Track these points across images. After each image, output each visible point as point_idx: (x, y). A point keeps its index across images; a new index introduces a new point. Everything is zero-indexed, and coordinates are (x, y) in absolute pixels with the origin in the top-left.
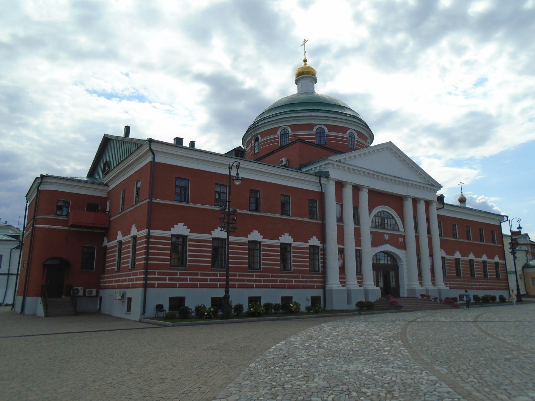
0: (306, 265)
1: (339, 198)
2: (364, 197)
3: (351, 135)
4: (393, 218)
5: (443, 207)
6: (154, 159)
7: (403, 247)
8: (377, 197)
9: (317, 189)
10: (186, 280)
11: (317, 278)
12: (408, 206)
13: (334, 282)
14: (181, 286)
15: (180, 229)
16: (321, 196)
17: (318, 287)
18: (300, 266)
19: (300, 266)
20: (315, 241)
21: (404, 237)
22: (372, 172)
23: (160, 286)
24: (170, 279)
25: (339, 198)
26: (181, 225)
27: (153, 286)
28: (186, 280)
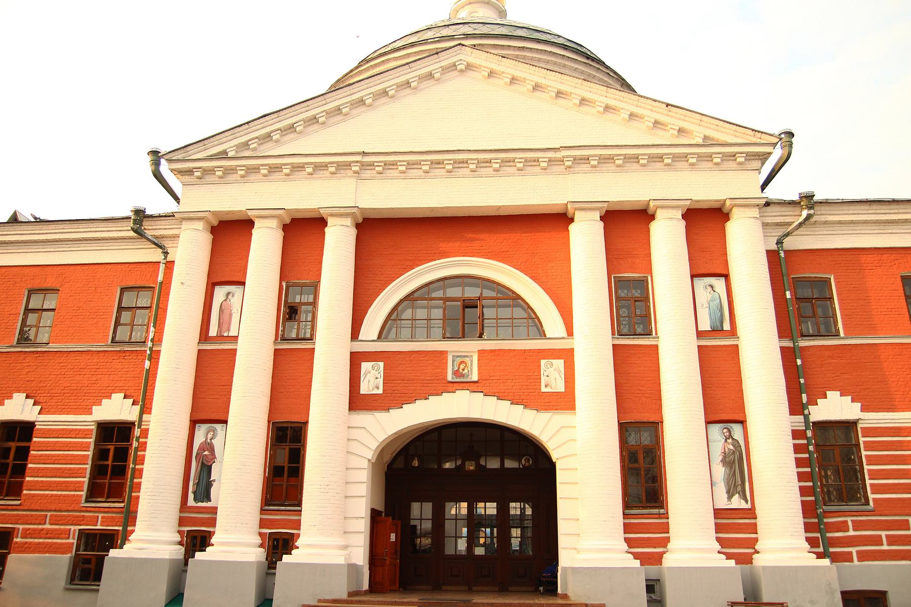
2: (339, 243)
4: (515, 299)
7: (564, 401)
8: (384, 237)
9: (155, 255)
12: (586, 241)
20: (116, 408)
22: (359, 158)
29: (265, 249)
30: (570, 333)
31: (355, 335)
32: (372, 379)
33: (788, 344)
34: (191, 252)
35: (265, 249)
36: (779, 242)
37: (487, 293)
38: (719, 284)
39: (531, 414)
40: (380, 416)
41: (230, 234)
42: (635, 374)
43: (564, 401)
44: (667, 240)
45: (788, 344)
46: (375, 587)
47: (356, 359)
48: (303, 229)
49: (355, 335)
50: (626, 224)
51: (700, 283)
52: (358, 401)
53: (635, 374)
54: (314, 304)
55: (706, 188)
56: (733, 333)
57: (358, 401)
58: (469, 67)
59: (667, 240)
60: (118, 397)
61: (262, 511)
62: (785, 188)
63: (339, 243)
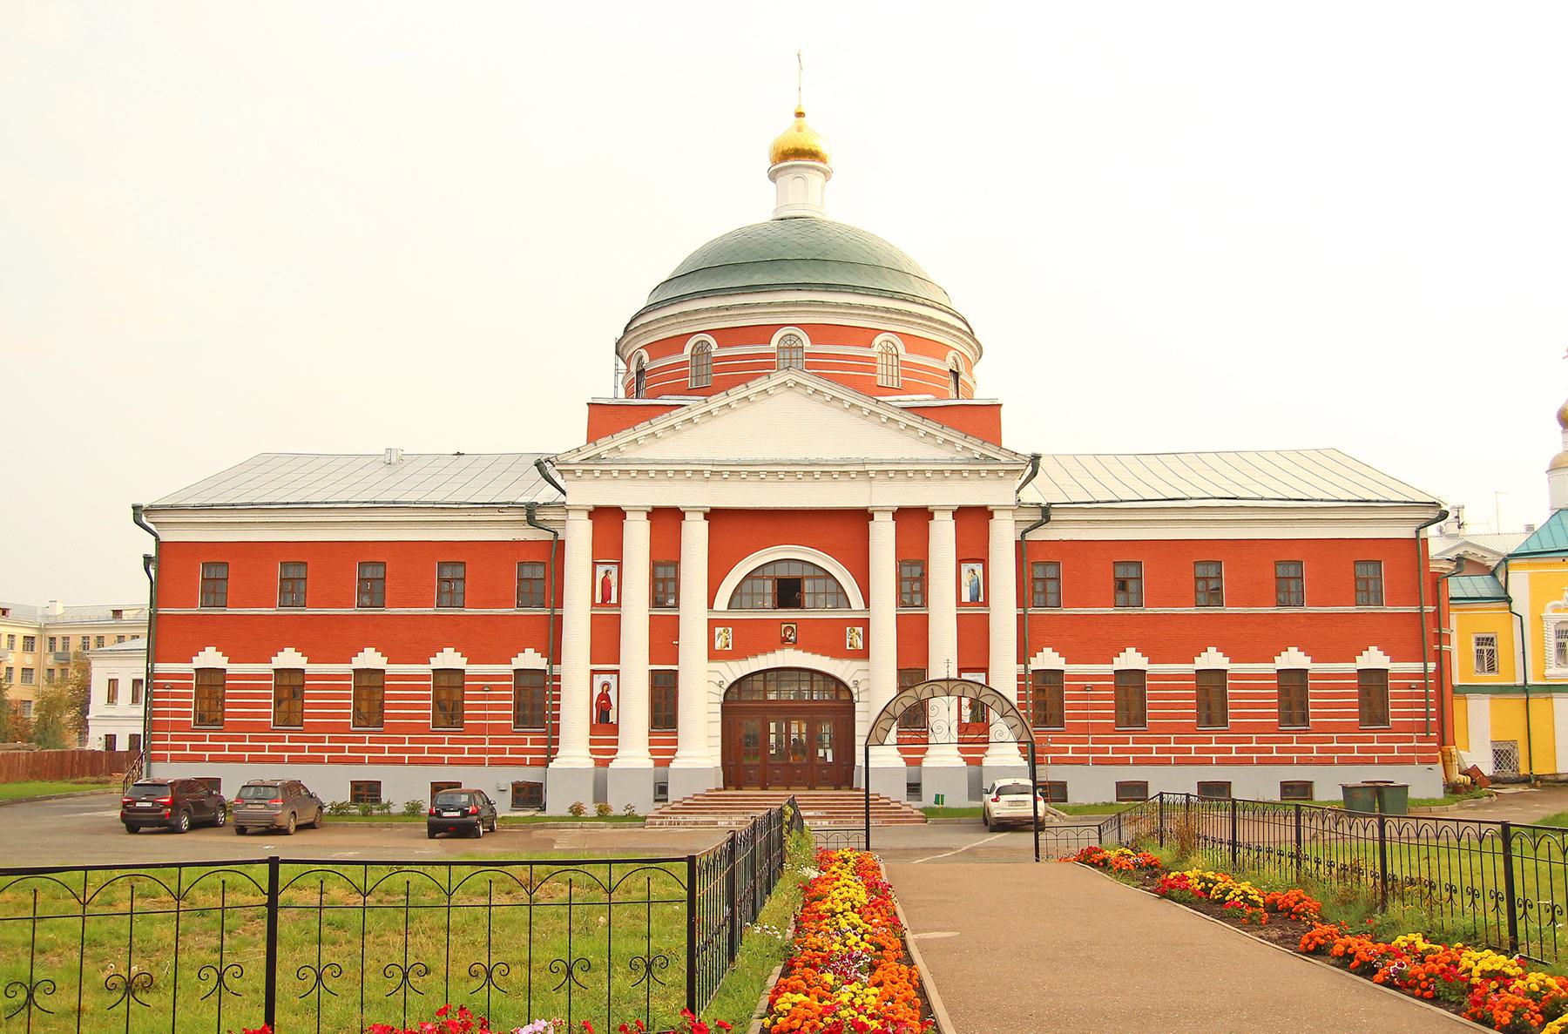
0: (506, 715)
1: (609, 544)
2: (695, 535)
3: (791, 347)
4: (829, 575)
5: (1048, 520)
6: (157, 539)
8: (731, 527)
10: (262, 749)
11: (533, 742)
12: (883, 535)
13: (575, 750)
14: (213, 759)
15: (211, 658)
16: (557, 548)
17: (534, 763)
18: (484, 717)
19: (484, 717)
20: (531, 659)
21: (865, 623)
23: (175, 759)
24: (193, 748)
25: (609, 544)
26: (210, 650)
27: (163, 759)
28: (262, 749)
29: (637, 535)
30: (867, 605)
31: (711, 605)
32: (723, 639)
33: (1021, 611)
34: (579, 537)
35: (637, 535)
36: (1023, 534)
37: (808, 571)
38: (979, 568)
39: (836, 662)
40: (732, 664)
41: (608, 519)
42: (913, 633)
43: (864, 654)
44: (943, 535)
45: (1021, 611)
46: (728, 783)
47: (712, 624)
48: (666, 519)
49: (711, 605)
50: (913, 520)
51: (965, 568)
52: (714, 655)
53: (913, 633)
54: (676, 580)
55: (972, 494)
56: (986, 603)
57: (714, 655)
58: (797, 384)
59: (943, 535)
60: (529, 651)
61: (650, 734)
62: (1031, 495)
63: (695, 535)
